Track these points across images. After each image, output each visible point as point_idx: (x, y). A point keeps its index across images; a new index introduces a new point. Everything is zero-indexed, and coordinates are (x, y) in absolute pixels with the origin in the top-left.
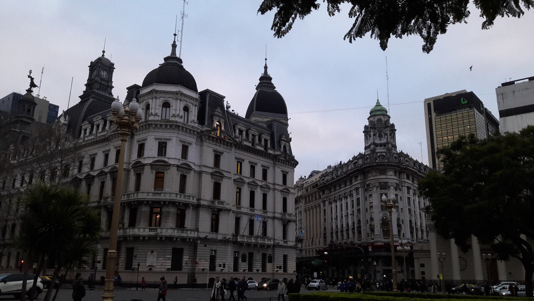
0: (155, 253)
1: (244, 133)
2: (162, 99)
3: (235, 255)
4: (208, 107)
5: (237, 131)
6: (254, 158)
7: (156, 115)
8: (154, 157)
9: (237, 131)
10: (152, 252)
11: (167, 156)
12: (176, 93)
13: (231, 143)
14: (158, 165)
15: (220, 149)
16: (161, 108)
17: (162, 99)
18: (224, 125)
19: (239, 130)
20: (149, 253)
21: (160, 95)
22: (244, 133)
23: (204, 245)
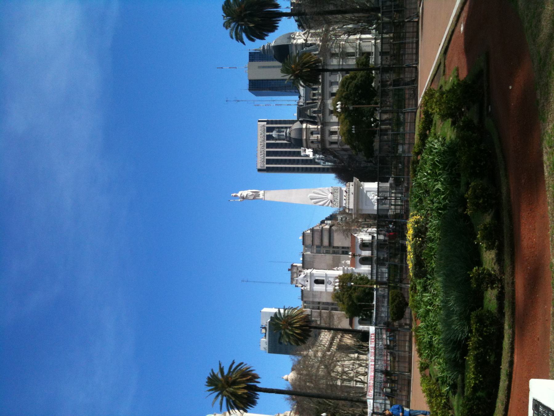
1: (314, 92)
2: (310, 144)
5: (315, 97)
6: (327, 84)
7: (318, 146)
13: (323, 104)
15: (327, 112)
17: (310, 144)
22: (314, 92)
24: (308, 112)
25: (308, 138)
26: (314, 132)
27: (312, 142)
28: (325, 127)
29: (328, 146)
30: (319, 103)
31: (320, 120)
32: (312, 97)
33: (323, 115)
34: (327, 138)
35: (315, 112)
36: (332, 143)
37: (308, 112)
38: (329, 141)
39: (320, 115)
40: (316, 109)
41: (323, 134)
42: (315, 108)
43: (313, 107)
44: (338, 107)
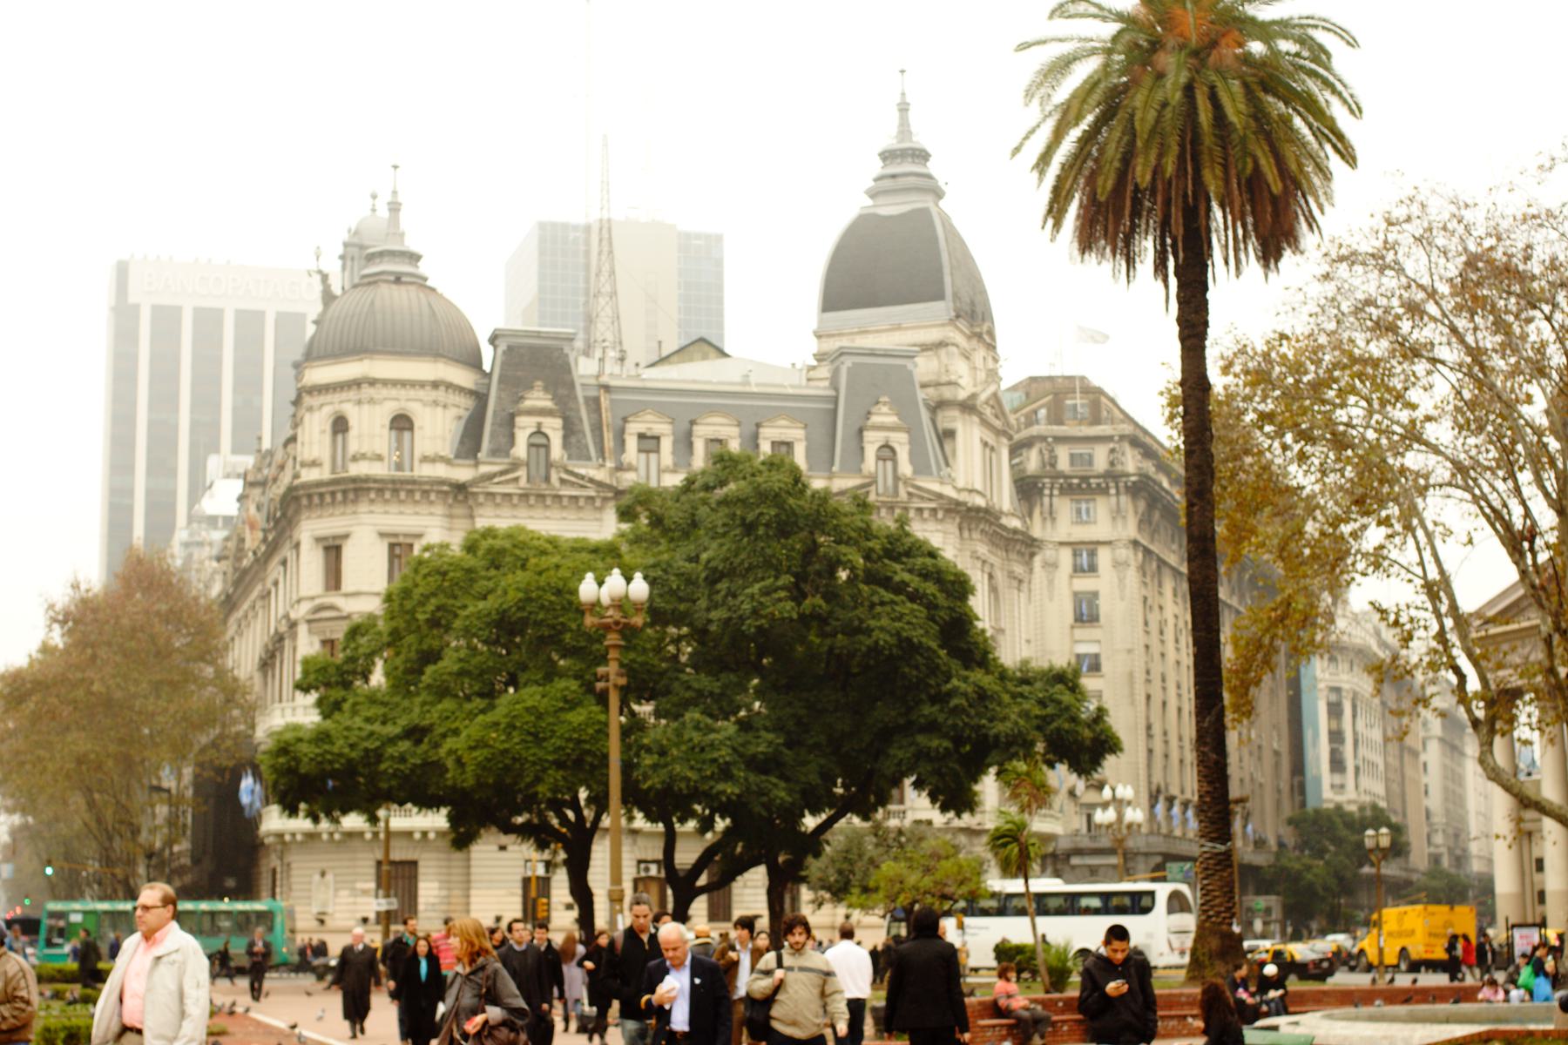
0: (329, 877)
1: (666, 445)
2: (327, 410)
3: (647, 870)
4: (499, 389)
5: (632, 443)
7: (314, 464)
8: (312, 598)
9: (632, 443)
10: (323, 874)
11: (348, 584)
12: (356, 384)
14: (320, 620)
16: (327, 438)
18: (566, 438)
19: (642, 436)
20: (317, 877)
21: (322, 399)
22: (666, 445)
23: (495, 848)
24: (538, 398)
25: (367, 391)
26: (407, 435)
27: (340, 425)
28: (439, 509)
29: (310, 529)
30: (600, 475)
31: (490, 477)
32: (634, 428)
33: (524, 496)
34: (366, 518)
35: (539, 442)
36: (333, 551)
37: (538, 398)
38: (346, 536)
39: (522, 473)
40: (557, 451)
41: (395, 491)
42: (566, 444)
43: (570, 430)
44: (615, 581)
